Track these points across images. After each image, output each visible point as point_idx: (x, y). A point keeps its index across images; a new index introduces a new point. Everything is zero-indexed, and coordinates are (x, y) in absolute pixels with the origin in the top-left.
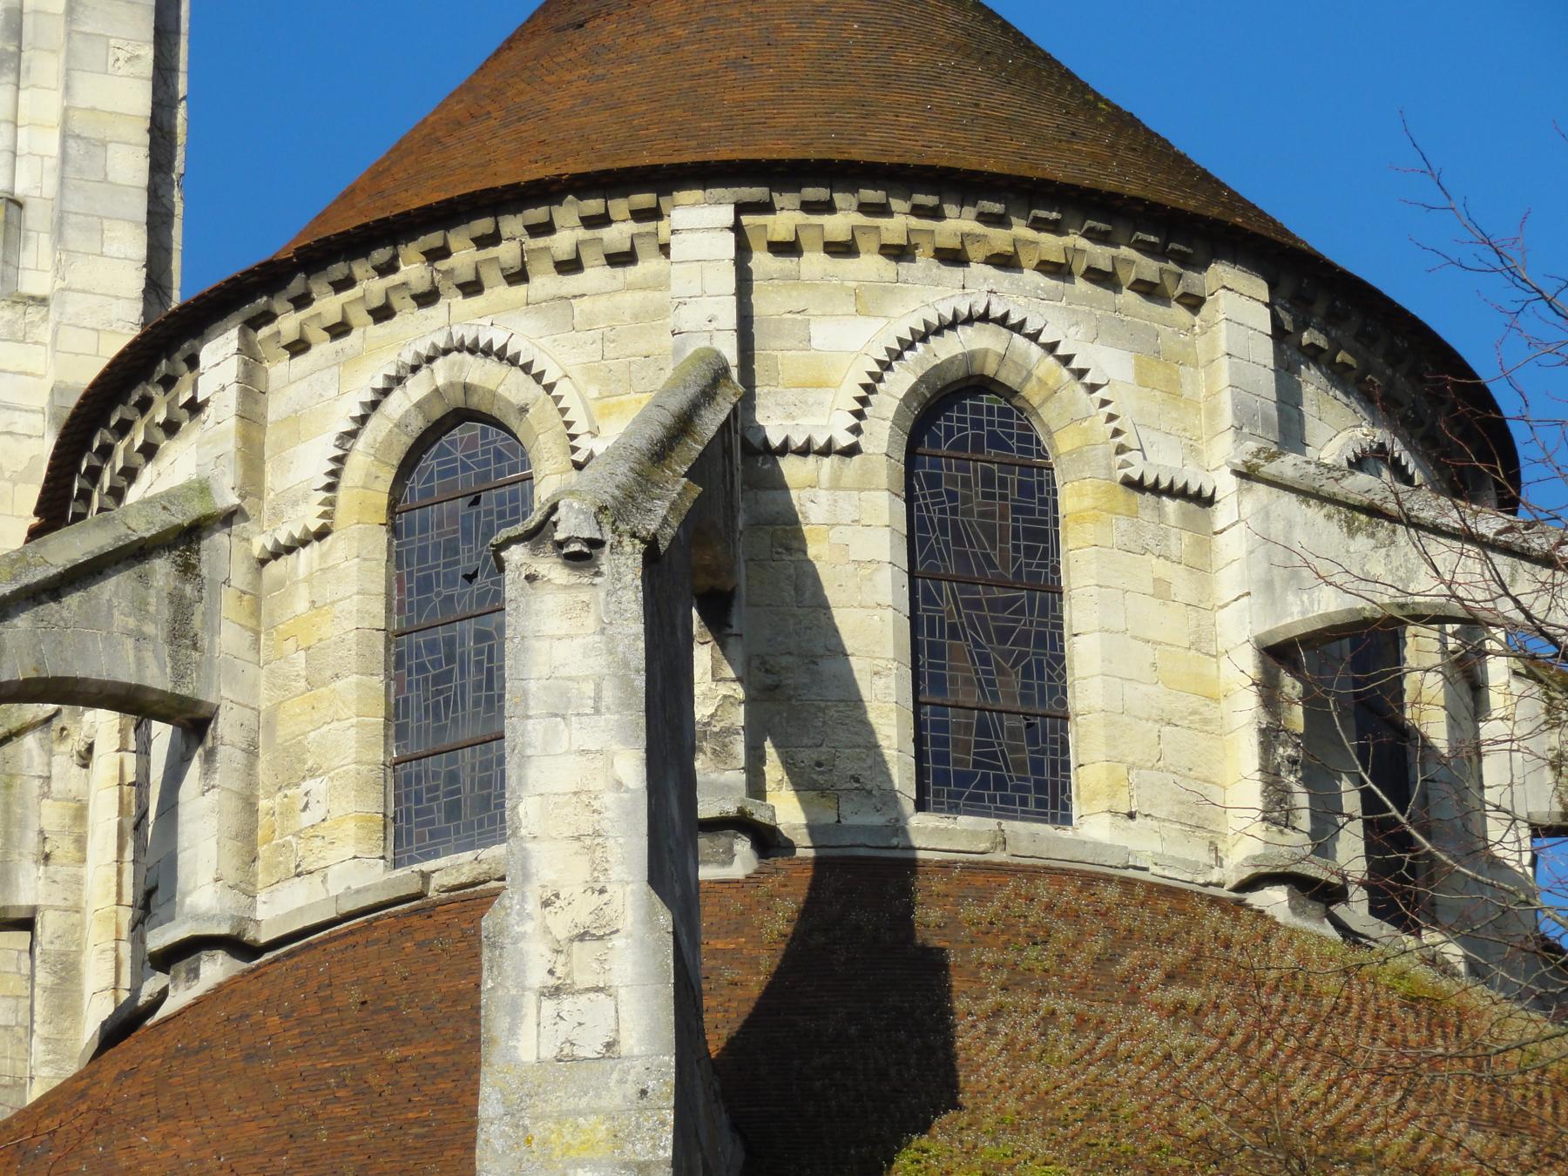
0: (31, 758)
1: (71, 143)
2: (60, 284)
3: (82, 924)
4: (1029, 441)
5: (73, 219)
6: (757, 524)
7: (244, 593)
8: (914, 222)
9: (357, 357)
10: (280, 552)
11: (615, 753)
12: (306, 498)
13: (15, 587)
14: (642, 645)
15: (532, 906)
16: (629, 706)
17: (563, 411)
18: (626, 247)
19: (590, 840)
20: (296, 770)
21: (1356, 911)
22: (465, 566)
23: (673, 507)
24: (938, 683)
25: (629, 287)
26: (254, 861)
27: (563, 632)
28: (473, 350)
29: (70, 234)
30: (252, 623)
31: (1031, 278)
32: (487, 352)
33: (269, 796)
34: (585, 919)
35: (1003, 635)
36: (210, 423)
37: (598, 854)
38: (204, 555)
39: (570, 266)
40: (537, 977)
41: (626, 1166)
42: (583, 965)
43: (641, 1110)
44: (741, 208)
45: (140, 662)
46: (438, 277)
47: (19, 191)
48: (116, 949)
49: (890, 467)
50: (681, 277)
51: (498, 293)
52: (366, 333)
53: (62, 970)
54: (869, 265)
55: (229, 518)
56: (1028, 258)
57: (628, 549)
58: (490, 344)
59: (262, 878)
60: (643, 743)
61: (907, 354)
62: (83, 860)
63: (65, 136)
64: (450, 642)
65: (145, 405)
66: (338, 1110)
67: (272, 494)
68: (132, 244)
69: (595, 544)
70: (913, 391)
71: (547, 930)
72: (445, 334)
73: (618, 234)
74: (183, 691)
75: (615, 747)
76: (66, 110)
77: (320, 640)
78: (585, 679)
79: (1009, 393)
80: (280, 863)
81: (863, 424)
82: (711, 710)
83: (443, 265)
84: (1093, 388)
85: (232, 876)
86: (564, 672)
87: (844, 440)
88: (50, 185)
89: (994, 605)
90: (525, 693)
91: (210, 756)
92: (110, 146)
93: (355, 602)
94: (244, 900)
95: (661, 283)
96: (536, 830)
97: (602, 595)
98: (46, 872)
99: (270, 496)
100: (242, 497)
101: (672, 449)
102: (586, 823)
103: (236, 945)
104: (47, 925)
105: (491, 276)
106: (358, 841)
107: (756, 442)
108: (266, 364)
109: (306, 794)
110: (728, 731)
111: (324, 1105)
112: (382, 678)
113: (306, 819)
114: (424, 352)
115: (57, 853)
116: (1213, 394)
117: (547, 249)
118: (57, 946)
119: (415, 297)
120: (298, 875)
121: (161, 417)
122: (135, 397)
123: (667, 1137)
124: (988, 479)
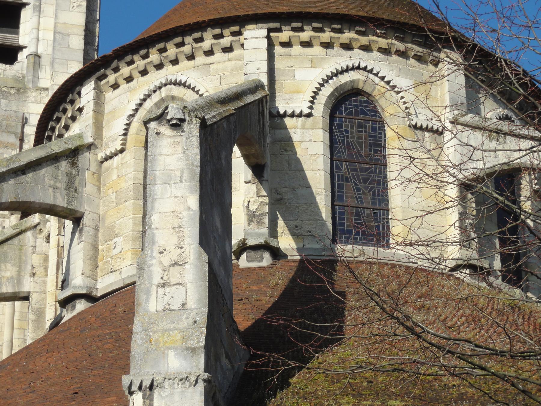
0: (29, 239)
1: (57, 35)
2: (52, 83)
3: (46, 297)
4: (375, 112)
5: (57, 61)
6: (275, 141)
7: (95, 173)
8: (333, 34)
9: (135, 89)
11: (188, 197)
13: (8, 168)
14: (199, 157)
15: (156, 254)
16: (193, 180)
18: (229, 45)
19: (178, 229)
20: (112, 235)
21: (498, 282)
23: (220, 114)
24: (341, 198)
25: (230, 60)
26: (97, 268)
27: (169, 153)
28: (175, 83)
29: (56, 66)
30: (97, 184)
31: (376, 54)
32: (180, 84)
33: (103, 244)
34: (175, 258)
35: (365, 181)
37: (181, 234)
38: (80, 159)
39: (209, 53)
40: (157, 280)
41: (187, 349)
42: (174, 275)
43: (194, 329)
44: (270, 31)
45: (55, 197)
46: (163, 59)
47: (39, 52)
49: (323, 121)
50: (247, 54)
51: (184, 63)
52: (139, 80)
53: (39, 314)
54: (317, 50)
55: (89, 147)
56: (375, 47)
57: (194, 122)
58: (181, 81)
59: (100, 274)
60: (198, 192)
61: (330, 81)
63: (55, 33)
65: (65, 111)
66: (108, 346)
67: (106, 138)
69: (182, 120)
70: (332, 94)
71: (161, 263)
72: (165, 78)
73: (226, 41)
74: (71, 207)
75: (188, 195)
76: (55, 23)
77: (121, 188)
78: (177, 170)
79: (368, 95)
80: (105, 268)
81: (313, 106)
82: (256, 207)
83: (164, 54)
84: (398, 93)
85: (88, 273)
86: (169, 168)
87: (306, 111)
89: (361, 170)
90: (155, 176)
91: (81, 230)
92: (71, 36)
93: (131, 176)
94: (93, 282)
95: (241, 58)
96: (157, 226)
97: (184, 139)
98: (33, 280)
99: (105, 140)
100: (95, 139)
101: (230, 102)
103: (88, 297)
104: (34, 298)
105: (181, 58)
106: (132, 259)
107: (275, 112)
108: (105, 93)
109: (115, 243)
110: (262, 214)
111: (103, 345)
112: (142, 201)
113: (115, 252)
114: (158, 85)
115: (38, 273)
116: (443, 95)
117: (201, 47)
118: (37, 305)
119: (155, 66)
120: (112, 272)
121: (69, 115)
122: (61, 108)
123: (203, 338)
124: (360, 126)
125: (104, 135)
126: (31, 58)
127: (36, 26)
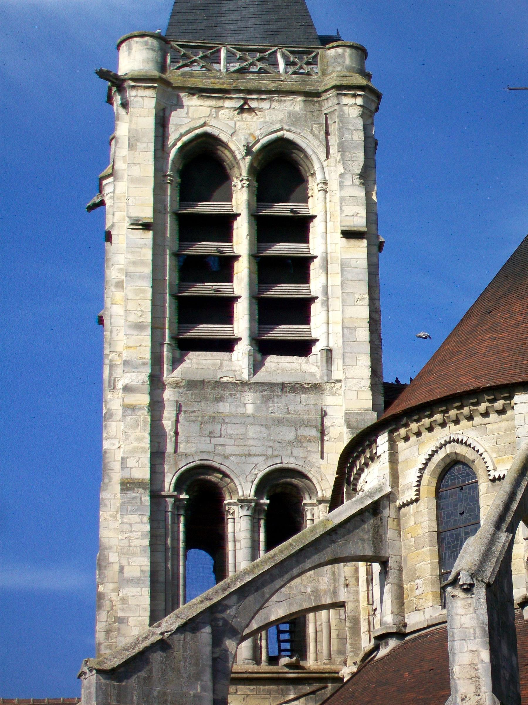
1: (345, 330)
5: (347, 355)
7: (395, 519)
9: (423, 443)
10: (404, 505)
11: (481, 651)
12: (411, 488)
17: (485, 463)
20: (414, 577)
22: (460, 510)
25: (503, 420)
26: (403, 605)
27: (463, 613)
28: (457, 441)
29: (346, 360)
36: (381, 463)
37: (477, 683)
39: (486, 415)
45: (363, 547)
46: (445, 418)
48: (369, 619)
53: (354, 621)
55: (389, 497)
62: (358, 585)
64: (457, 535)
67: (401, 486)
68: (366, 361)
69: (472, 585)
72: (449, 437)
75: (481, 649)
77: (418, 535)
78: (471, 628)
80: (411, 606)
85: (396, 611)
86: (464, 626)
88: (340, 344)
92: (357, 329)
94: (401, 618)
96: (458, 676)
97: (475, 601)
98: (347, 590)
99: (401, 486)
100: (392, 488)
102: (473, 674)
104: (350, 606)
106: (433, 601)
108: (397, 443)
109: (417, 584)
112: (437, 547)
113: (418, 592)
114: (443, 443)
115: (351, 583)
117: (477, 409)
118: (352, 614)
120: (416, 610)
125: (400, 482)
126: (324, 353)
127: (325, 320)
